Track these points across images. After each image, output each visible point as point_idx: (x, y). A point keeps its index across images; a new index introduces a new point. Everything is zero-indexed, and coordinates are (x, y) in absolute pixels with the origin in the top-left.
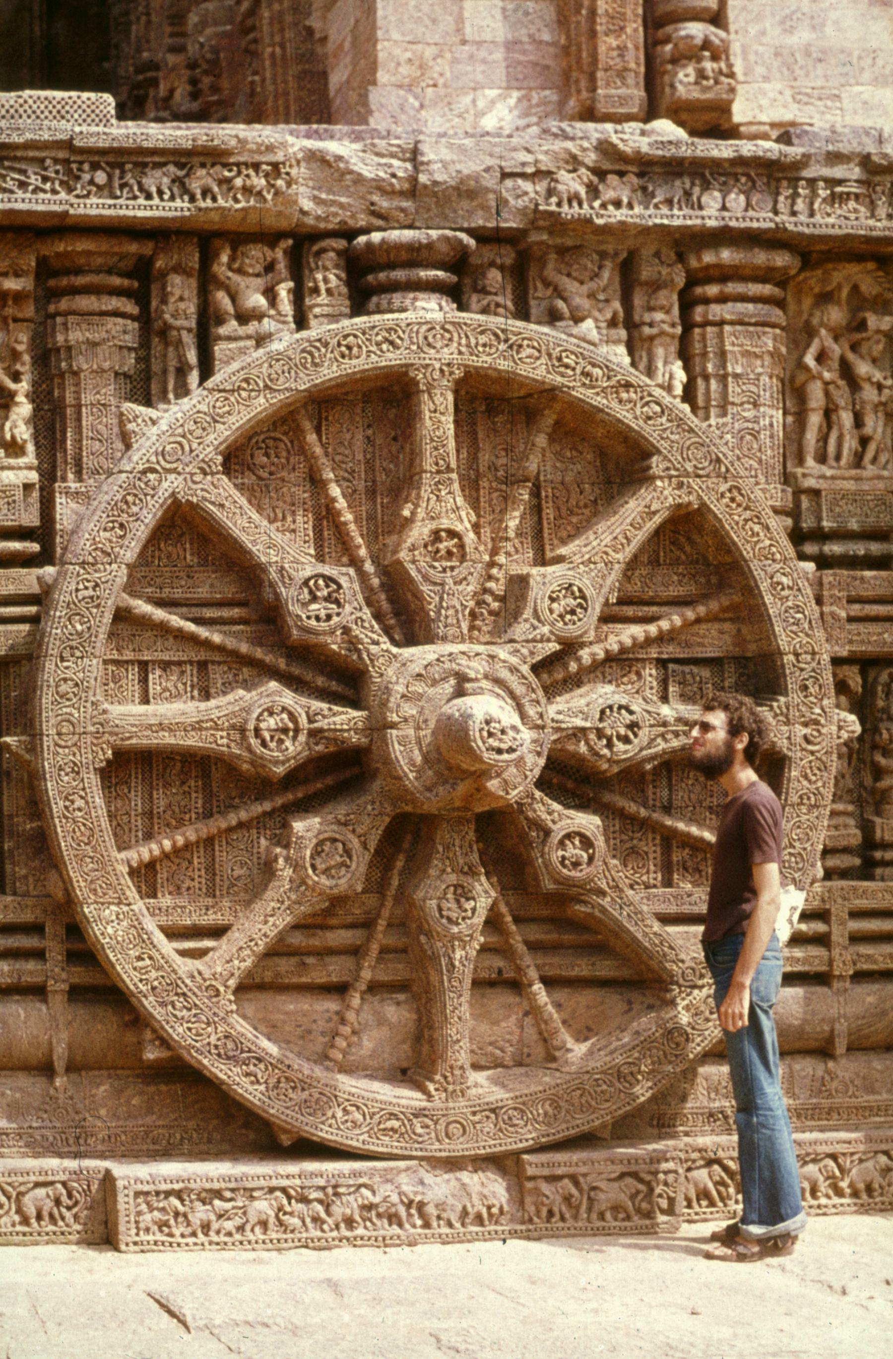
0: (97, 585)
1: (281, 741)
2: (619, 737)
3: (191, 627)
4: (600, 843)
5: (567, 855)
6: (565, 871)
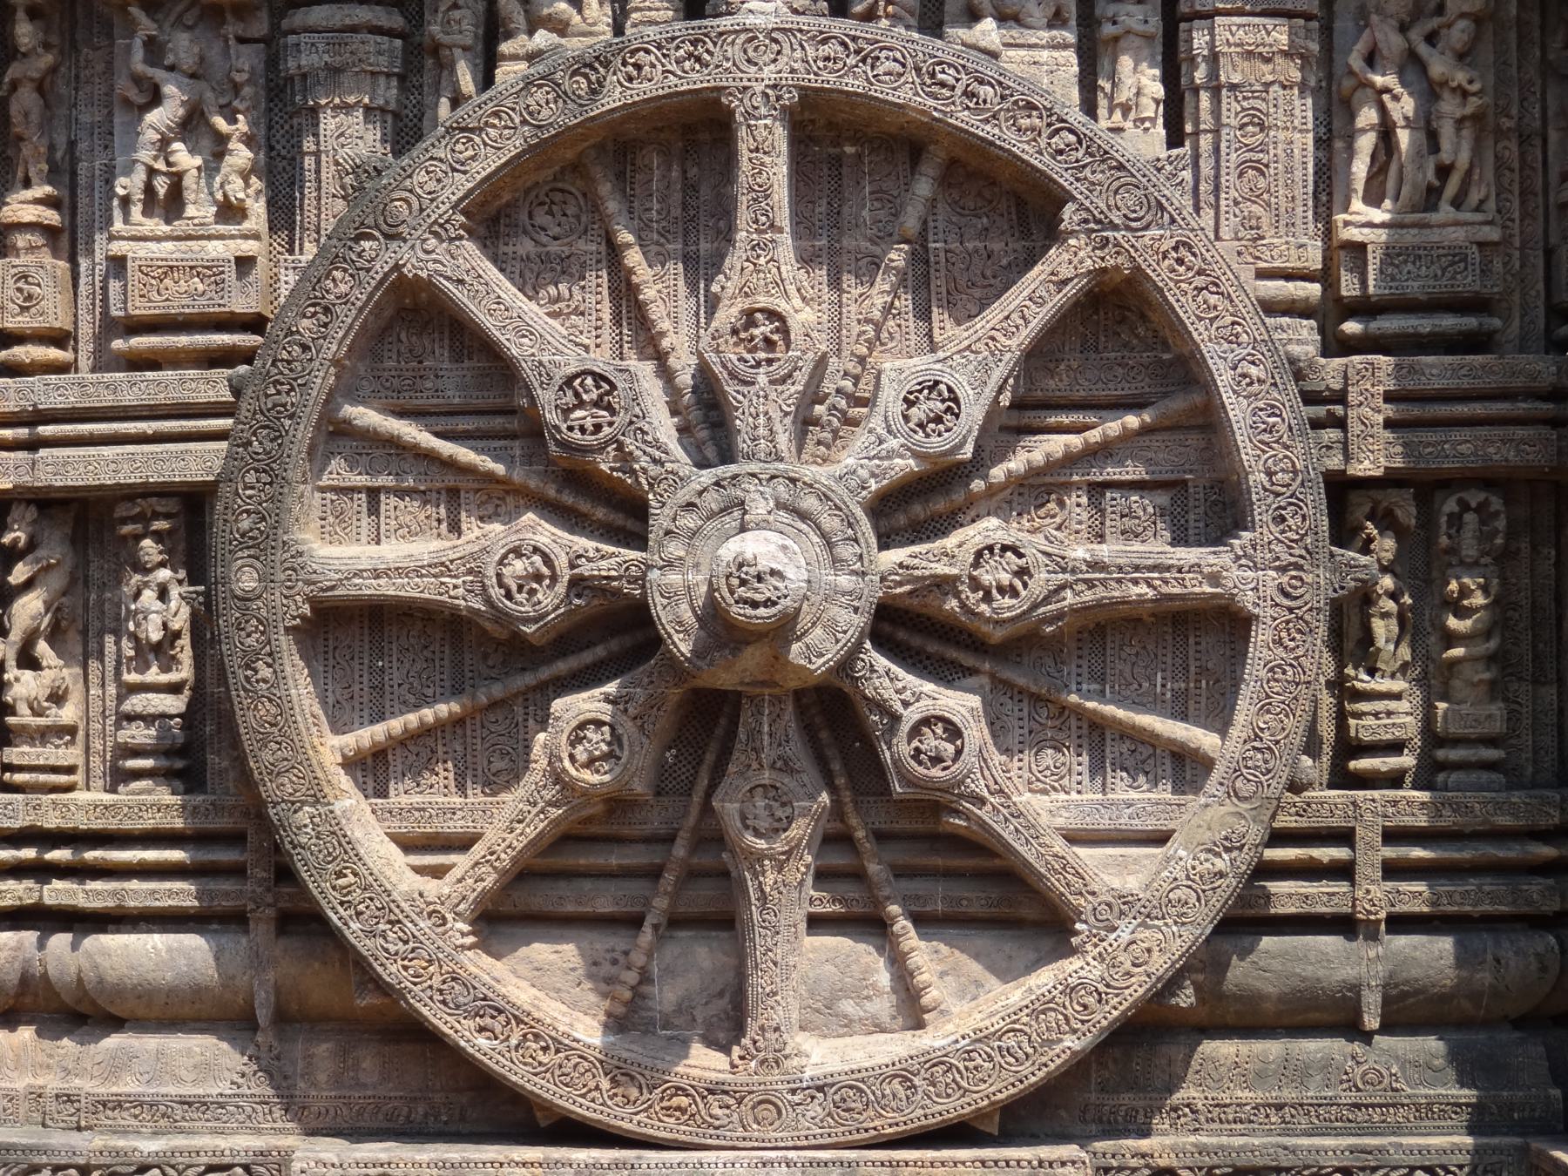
0: (292, 389)
1: (532, 592)
3: (426, 439)
4: (976, 734)
5: (923, 747)
6: (921, 769)
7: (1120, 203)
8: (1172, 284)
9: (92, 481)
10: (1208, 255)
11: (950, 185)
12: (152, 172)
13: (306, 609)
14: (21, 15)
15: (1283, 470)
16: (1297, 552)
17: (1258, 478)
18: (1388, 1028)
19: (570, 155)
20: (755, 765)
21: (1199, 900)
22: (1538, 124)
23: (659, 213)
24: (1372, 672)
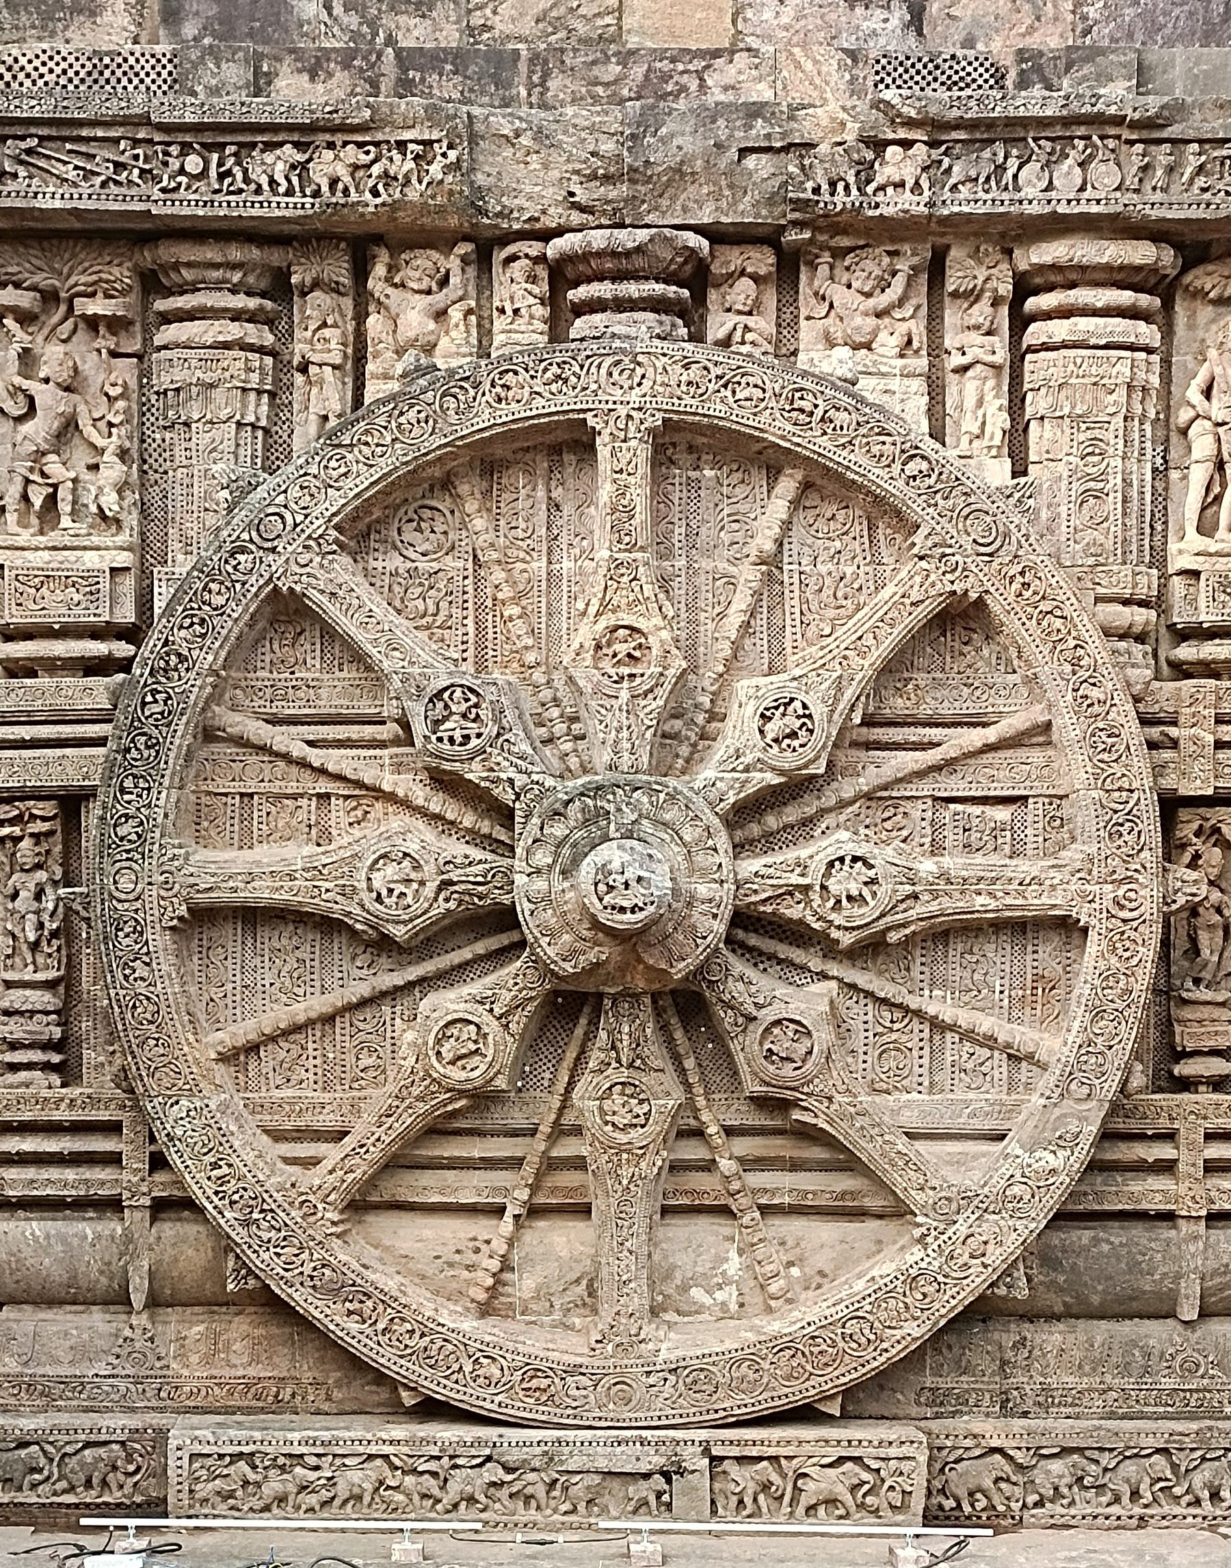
4: (823, 1036)
6: (772, 1068)
12: (28, 481)
13: (183, 910)
15: (1120, 789)
16: (1134, 867)
20: (614, 1064)
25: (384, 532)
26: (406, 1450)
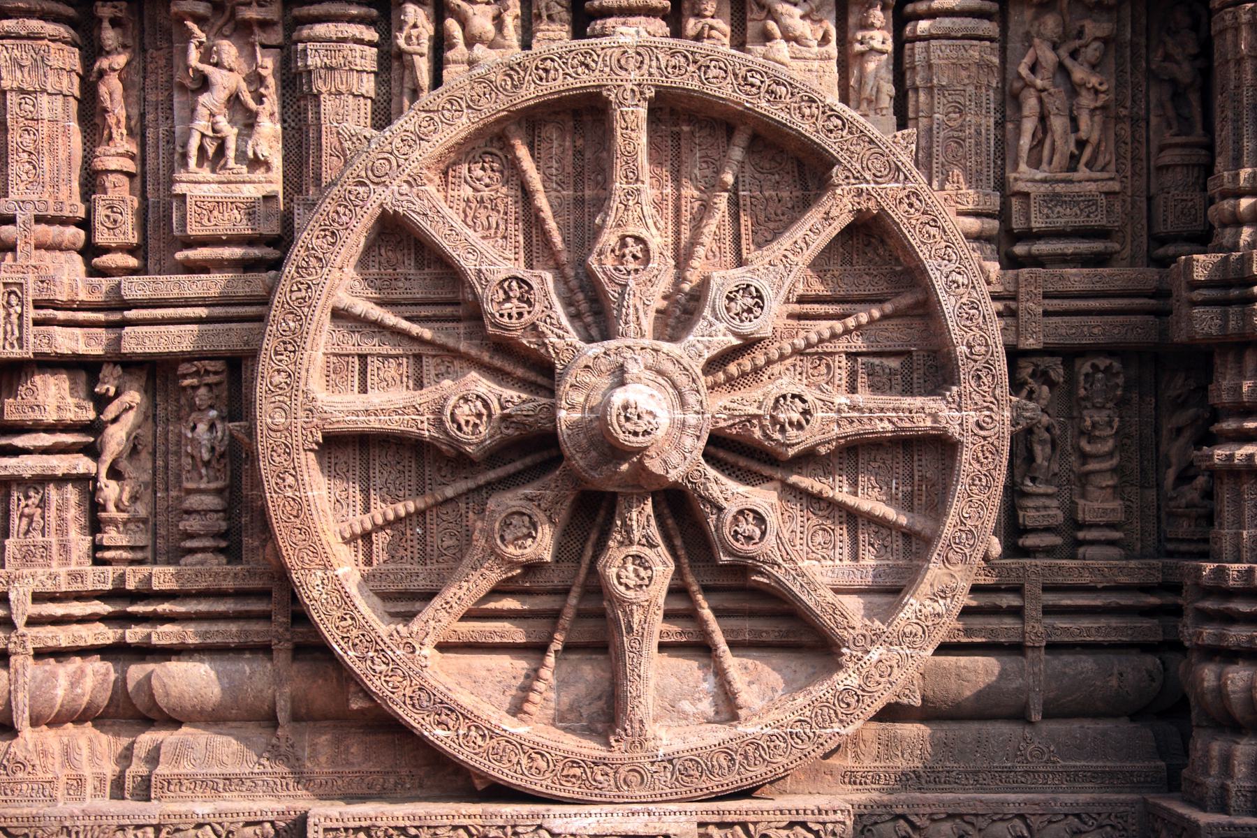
1: (476, 425)
2: (791, 424)
5: (740, 530)
6: (735, 543)
7: (870, 166)
8: (905, 221)
9: (162, 349)
10: (929, 202)
11: (753, 152)
12: (203, 136)
14: (106, 24)
17: (962, 349)
18: (1047, 716)
19: (496, 129)
20: (627, 542)
21: (924, 632)
22: (1142, 113)
23: (557, 169)
24: (1033, 480)
25: (458, 170)
26: (479, 821)
